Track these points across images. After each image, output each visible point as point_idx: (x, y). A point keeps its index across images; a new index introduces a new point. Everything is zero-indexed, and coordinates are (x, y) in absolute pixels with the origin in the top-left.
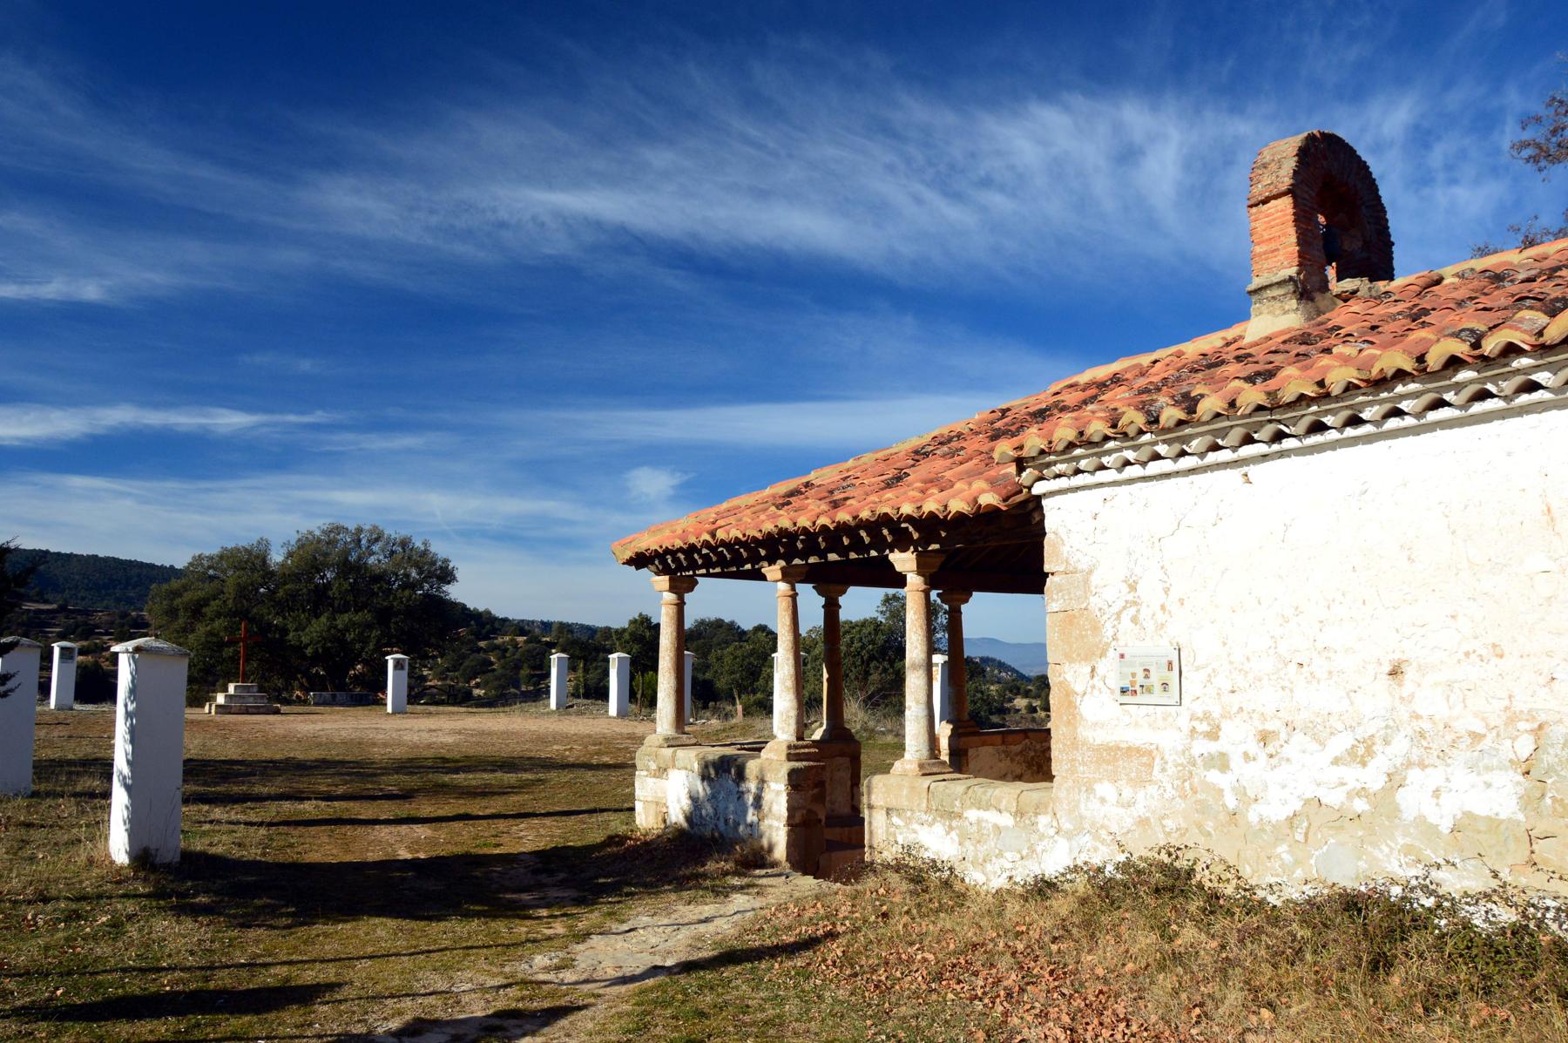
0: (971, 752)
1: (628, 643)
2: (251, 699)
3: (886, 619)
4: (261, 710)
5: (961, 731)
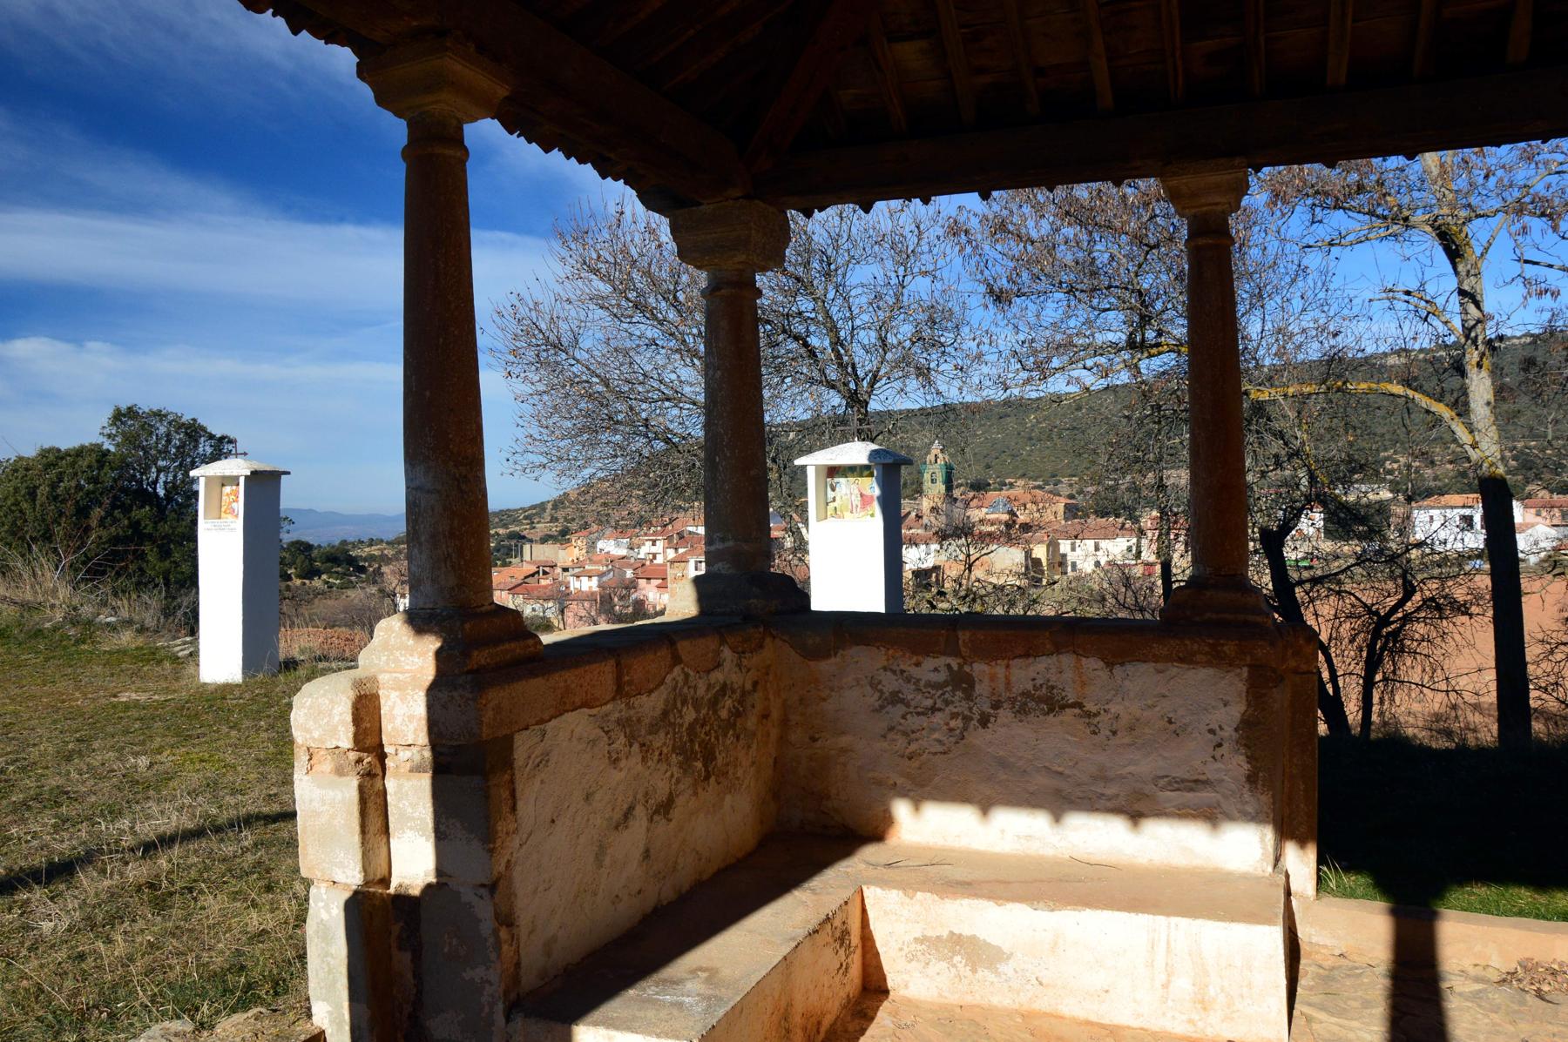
0: (524, 746)
3: (117, 445)
5: (481, 657)
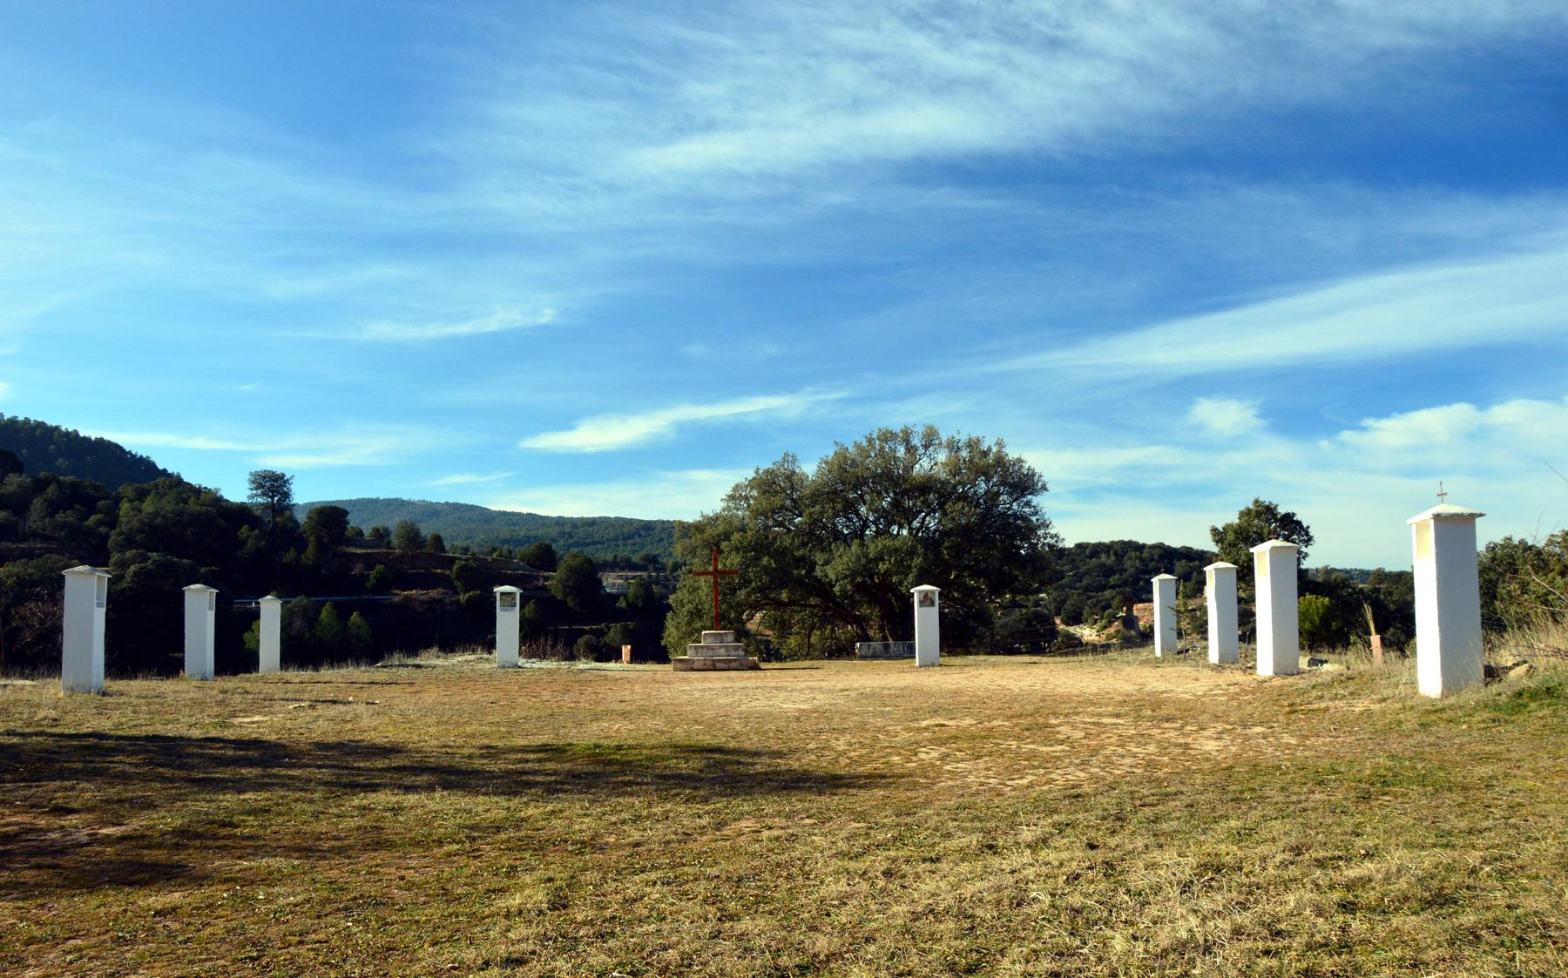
1: (1235, 545)
2: (722, 651)
4: (733, 665)
